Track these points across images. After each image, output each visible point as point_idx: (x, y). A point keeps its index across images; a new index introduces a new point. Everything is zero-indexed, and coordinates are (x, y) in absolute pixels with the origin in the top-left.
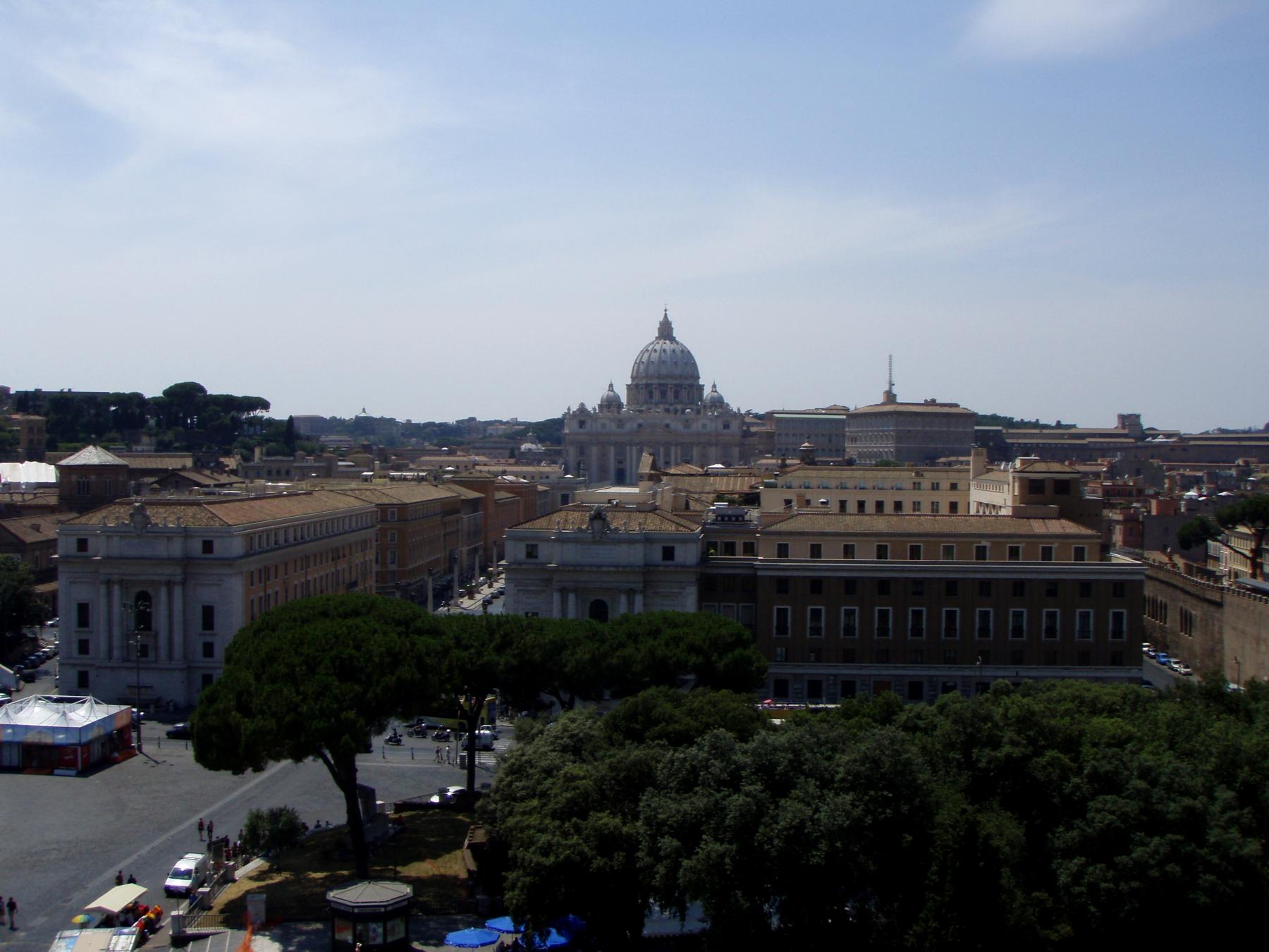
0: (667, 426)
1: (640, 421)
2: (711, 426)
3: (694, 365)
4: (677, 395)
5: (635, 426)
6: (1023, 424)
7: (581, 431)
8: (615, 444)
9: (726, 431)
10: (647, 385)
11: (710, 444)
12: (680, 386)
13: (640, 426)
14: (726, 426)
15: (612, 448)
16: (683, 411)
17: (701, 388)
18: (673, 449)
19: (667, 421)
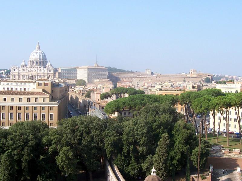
0: (36, 71)
1: (29, 70)
3: (45, 56)
4: (40, 63)
5: (28, 71)
6: (128, 72)
7: (14, 72)
8: (23, 75)
10: (33, 61)
13: (29, 71)
14: (50, 71)
15: (22, 76)
17: (47, 62)
18: (37, 76)
19: (35, 70)
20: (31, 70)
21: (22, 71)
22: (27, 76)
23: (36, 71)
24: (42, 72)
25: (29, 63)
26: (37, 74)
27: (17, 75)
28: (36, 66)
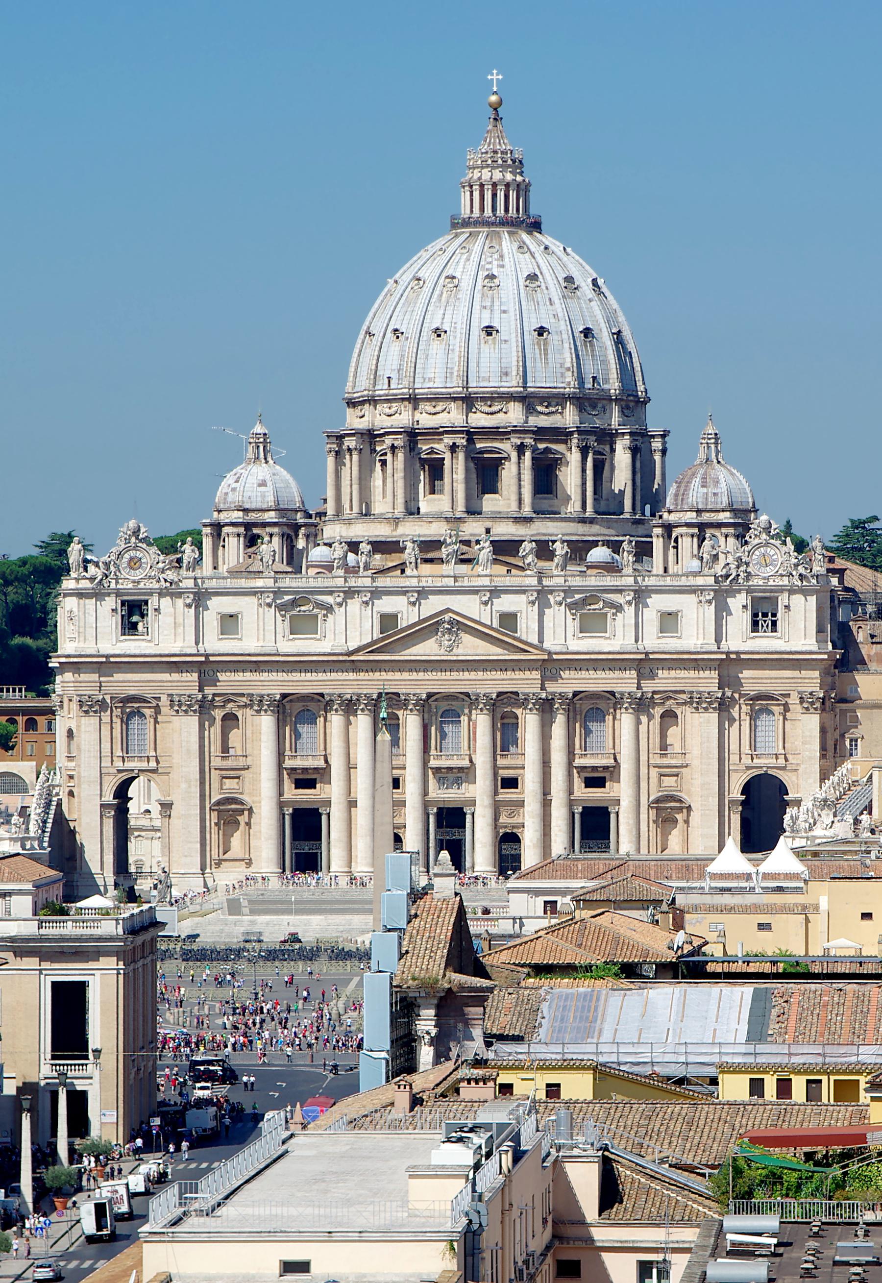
0: (509, 620)
2: (695, 632)
9: (765, 643)
11: (696, 701)
12: (560, 435)
13: (388, 621)
15: (266, 723)
16: (579, 550)
19: (506, 603)
20: (432, 605)
21: (261, 631)
22: (362, 722)
23: (509, 620)
24: (618, 637)
25: (352, 464)
26: (527, 682)
27: (178, 705)
28: (473, 528)
